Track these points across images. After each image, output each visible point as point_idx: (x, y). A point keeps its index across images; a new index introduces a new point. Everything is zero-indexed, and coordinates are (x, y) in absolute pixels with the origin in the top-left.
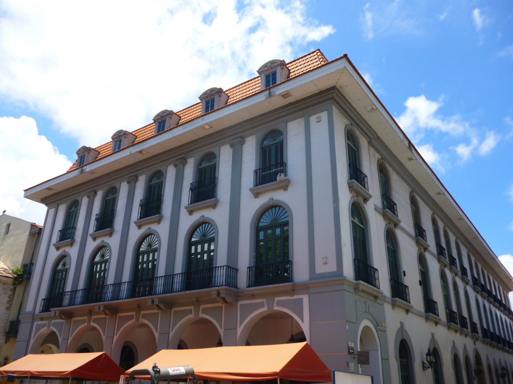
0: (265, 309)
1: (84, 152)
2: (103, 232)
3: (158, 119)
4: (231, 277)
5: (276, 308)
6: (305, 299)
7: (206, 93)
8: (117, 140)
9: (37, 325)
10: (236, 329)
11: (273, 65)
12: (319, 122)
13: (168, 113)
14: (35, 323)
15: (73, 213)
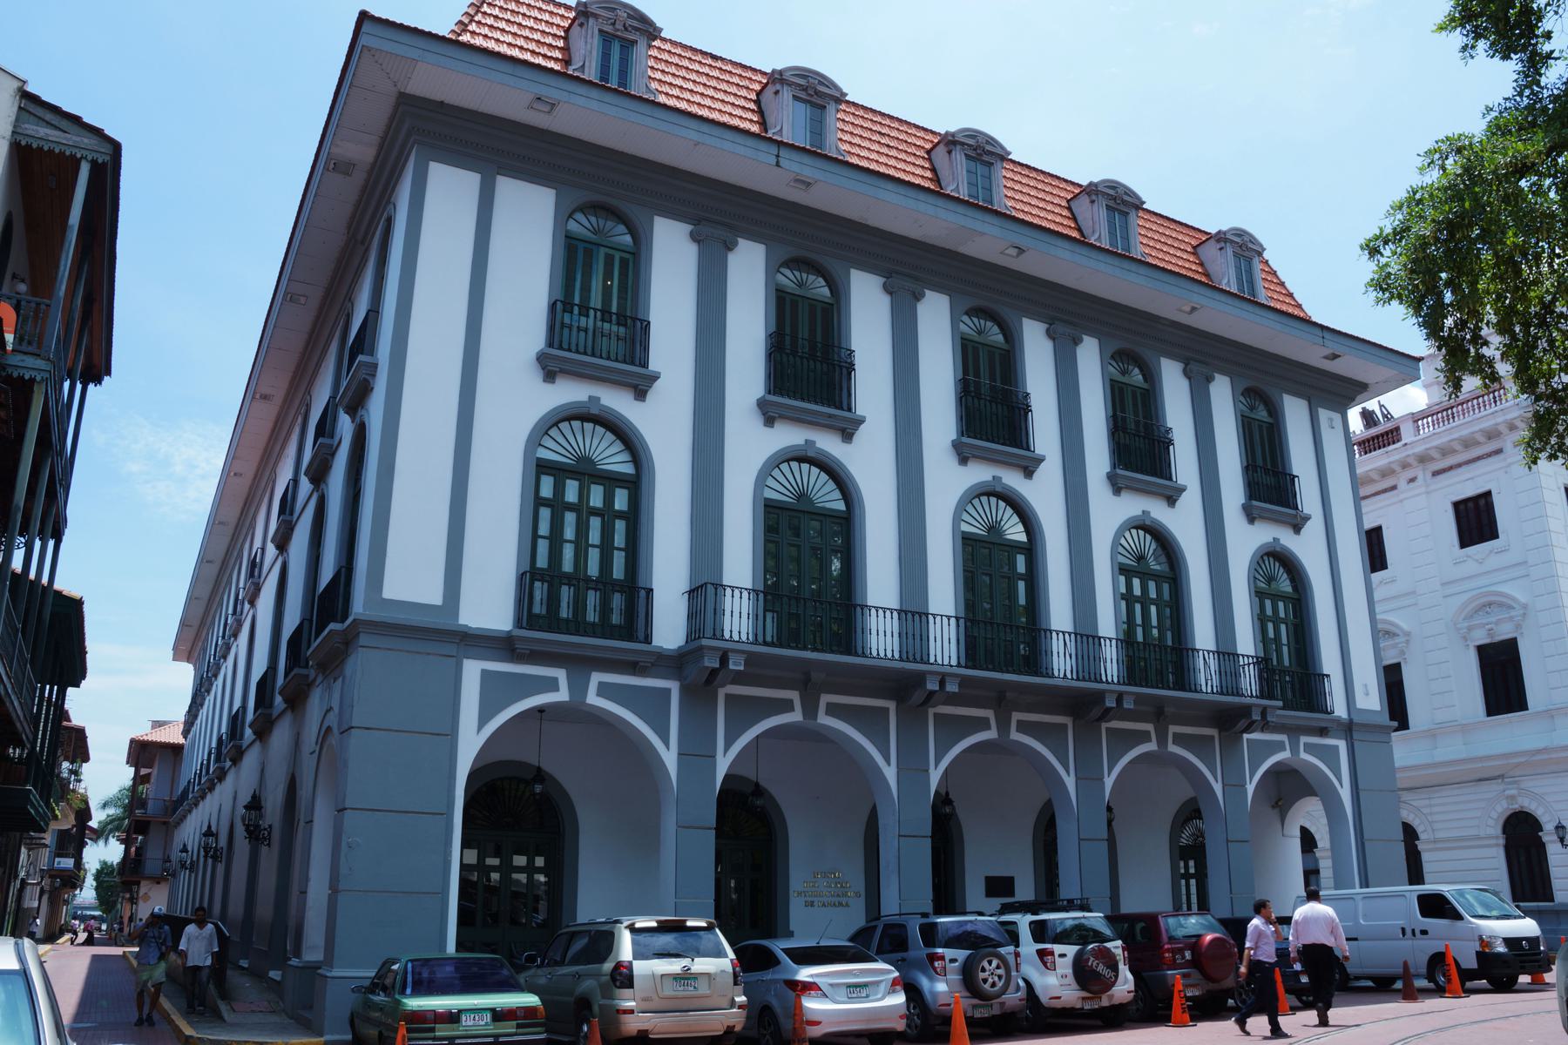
0: (1284, 755)
1: (626, 29)
2: (830, 416)
3: (967, 144)
4: (1092, 658)
5: (1304, 756)
6: (1342, 745)
7: (1113, 188)
8: (803, 95)
9: (484, 673)
10: (1243, 786)
11: (1250, 245)
12: (1333, 428)
13: (999, 151)
14: (472, 671)
15: (589, 256)
